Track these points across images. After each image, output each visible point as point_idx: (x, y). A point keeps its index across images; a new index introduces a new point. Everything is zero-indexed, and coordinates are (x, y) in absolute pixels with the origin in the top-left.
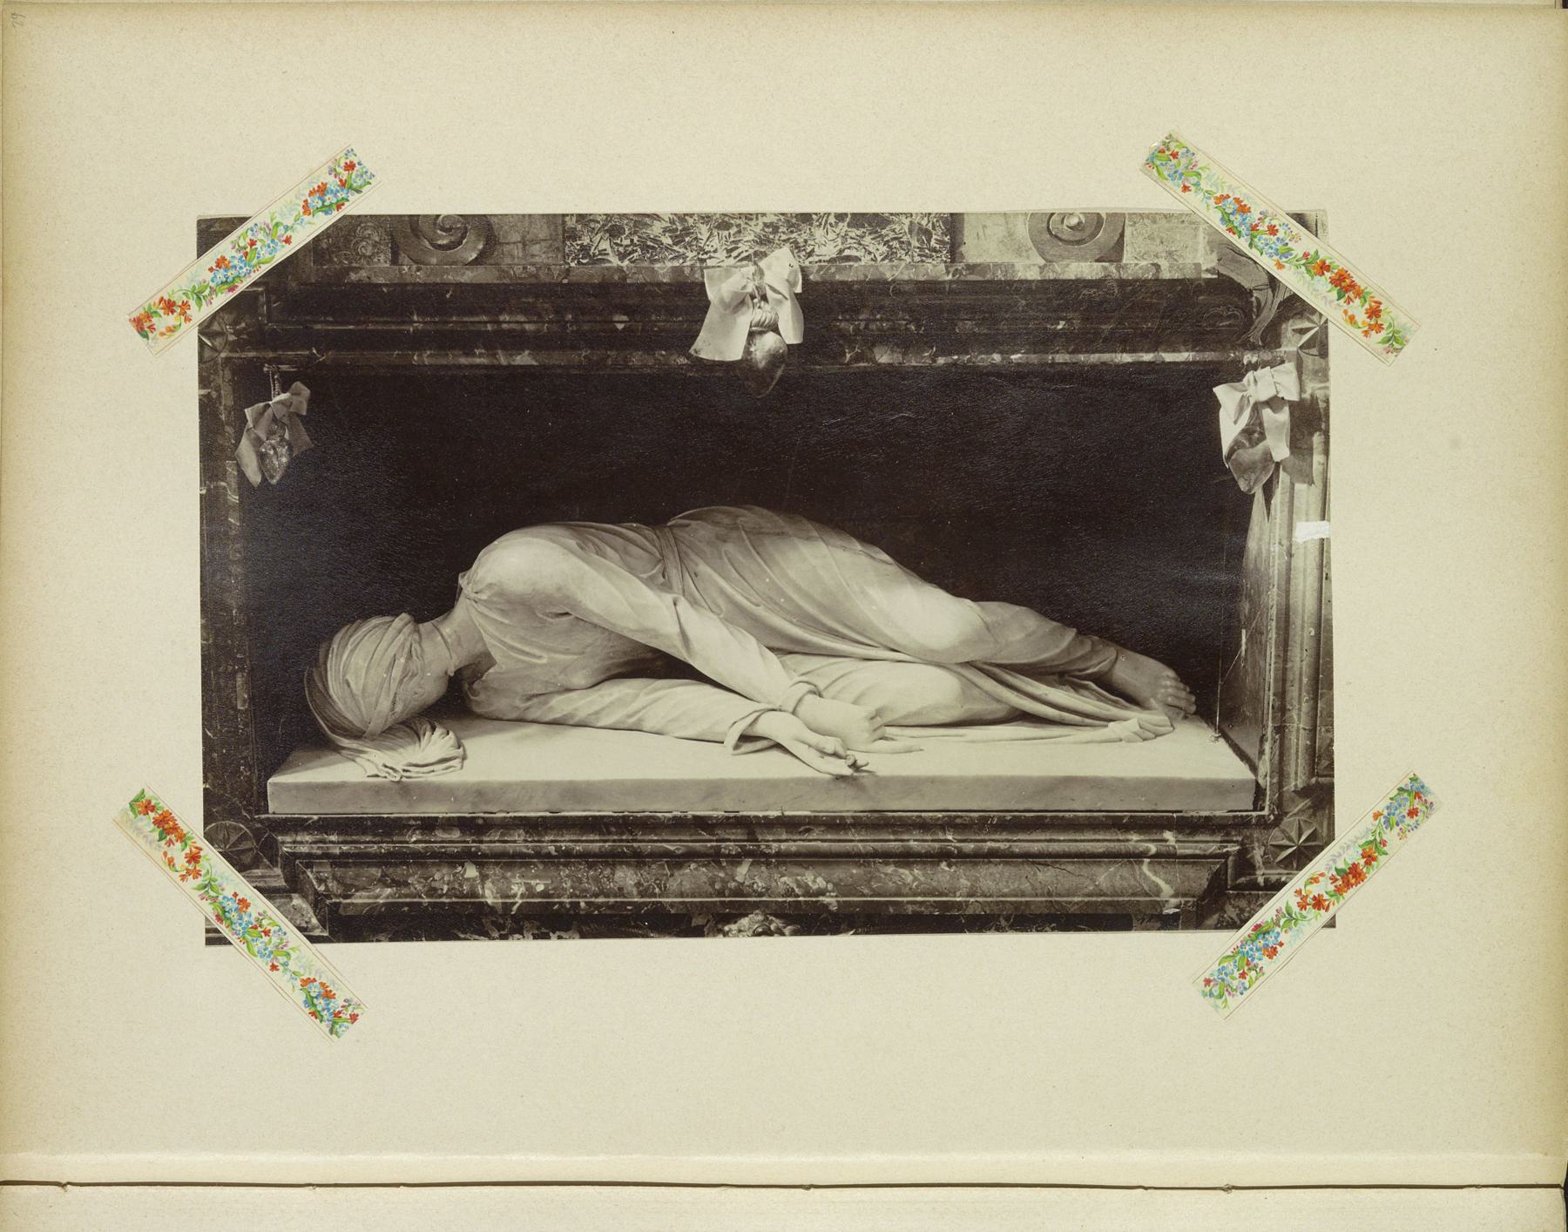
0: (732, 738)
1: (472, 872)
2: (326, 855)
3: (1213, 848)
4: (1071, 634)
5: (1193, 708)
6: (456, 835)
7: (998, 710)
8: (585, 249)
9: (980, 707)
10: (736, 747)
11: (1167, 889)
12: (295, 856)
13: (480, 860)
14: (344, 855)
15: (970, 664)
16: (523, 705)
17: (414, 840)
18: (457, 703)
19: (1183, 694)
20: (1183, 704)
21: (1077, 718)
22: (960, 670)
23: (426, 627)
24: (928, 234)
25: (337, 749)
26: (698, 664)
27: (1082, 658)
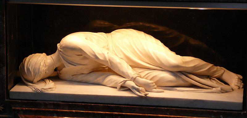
0: (118, 87)
2: (22, 110)
4: (211, 65)
5: (242, 86)
6: (52, 107)
7: (186, 84)
9: (181, 82)
10: (120, 89)
12: (14, 110)
14: (26, 110)
15: (180, 72)
16: (72, 77)
18: (56, 76)
19: (240, 83)
20: (239, 85)
21: (207, 87)
22: (176, 73)
23: (50, 56)
25: (27, 85)
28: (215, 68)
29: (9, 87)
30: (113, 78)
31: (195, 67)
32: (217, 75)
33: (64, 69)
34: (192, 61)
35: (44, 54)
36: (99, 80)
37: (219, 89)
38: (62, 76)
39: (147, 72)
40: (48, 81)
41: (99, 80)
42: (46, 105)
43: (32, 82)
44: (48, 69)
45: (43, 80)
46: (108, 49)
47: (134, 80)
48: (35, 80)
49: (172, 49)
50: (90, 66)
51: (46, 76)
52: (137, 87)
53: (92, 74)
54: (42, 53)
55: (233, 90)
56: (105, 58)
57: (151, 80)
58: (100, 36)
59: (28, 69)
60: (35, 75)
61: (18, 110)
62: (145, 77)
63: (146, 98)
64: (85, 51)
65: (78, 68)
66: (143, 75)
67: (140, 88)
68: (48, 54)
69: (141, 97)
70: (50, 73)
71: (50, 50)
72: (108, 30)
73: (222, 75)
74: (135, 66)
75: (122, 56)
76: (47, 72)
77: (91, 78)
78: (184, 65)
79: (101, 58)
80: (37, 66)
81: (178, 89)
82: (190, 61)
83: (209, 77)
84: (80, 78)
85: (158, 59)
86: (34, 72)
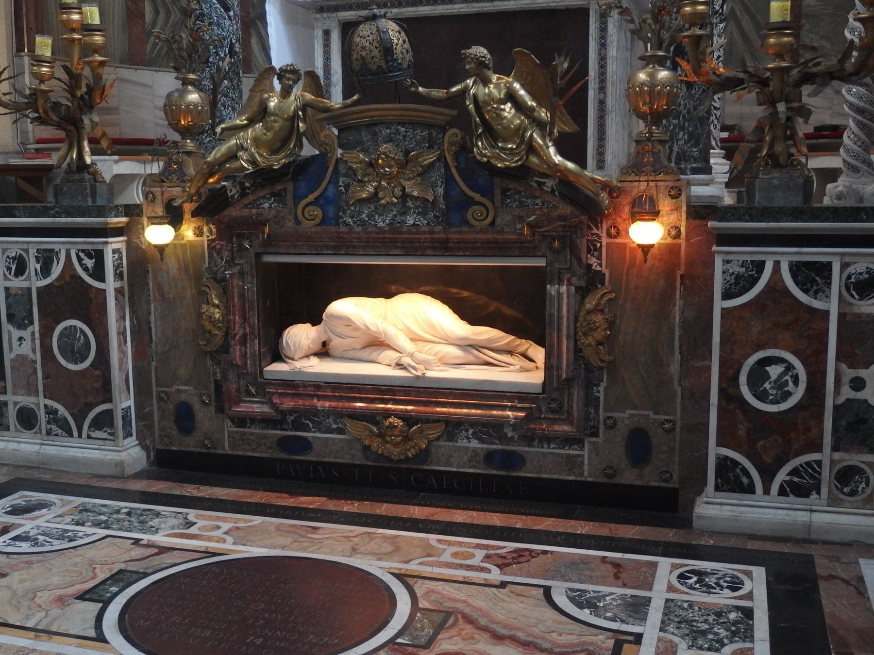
0: (393, 365)
1: (315, 401)
2: (277, 393)
3: (528, 405)
4: (512, 337)
6: (312, 389)
8: (345, 221)
9: (471, 358)
11: (511, 416)
13: (319, 398)
14: (282, 393)
17: (301, 391)
18: (324, 351)
24: (438, 217)
25: (286, 363)
26: (387, 342)
27: (518, 345)
28: (519, 341)
29: (262, 364)
30: (389, 355)
31: (489, 340)
32: (521, 349)
33: (332, 343)
34: (485, 332)
35: (308, 325)
36: (374, 356)
37: (518, 367)
38: (331, 352)
39: (430, 345)
40: (312, 358)
41: (374, 356)
42: (305, 386)
43: (293, 359)
44: (313, 342)
45: (307, 356)
46: (385, 318)
47: (411, 355)
48: (296, 357)
49: (463, 317)
50: (363, 340)
51: (310, 352)
52: (413, 364)
53: (366, 349)
54: (305, 323)
55: (537, 368)
56: (378, 328)
57: (435, 355)
58: (378, 303)
59: (287, 343)
60: (295, 350)
61: (273, 393)
62: (426, 352)
63: (423, 377)
64: (353, 320)
65: (349, 341)
66: (425, 349)
67: (417, 366)
68: (314, 324)
69: (418, 377)
70: (317, 347)
71: (316, 320)
72: (389, 295)
73: (527, 350)
74: (415, 339)
75: (401, 327)
76: (311, 346)
77: (365, 354)
78: (474, 337)
79: (373, 328)
80: (298, 340)
81: (467, 367)
82: (485, 333)
83: (510, 353)
84: (351, 354)
85: (442, 329)
86: (294, 347)
